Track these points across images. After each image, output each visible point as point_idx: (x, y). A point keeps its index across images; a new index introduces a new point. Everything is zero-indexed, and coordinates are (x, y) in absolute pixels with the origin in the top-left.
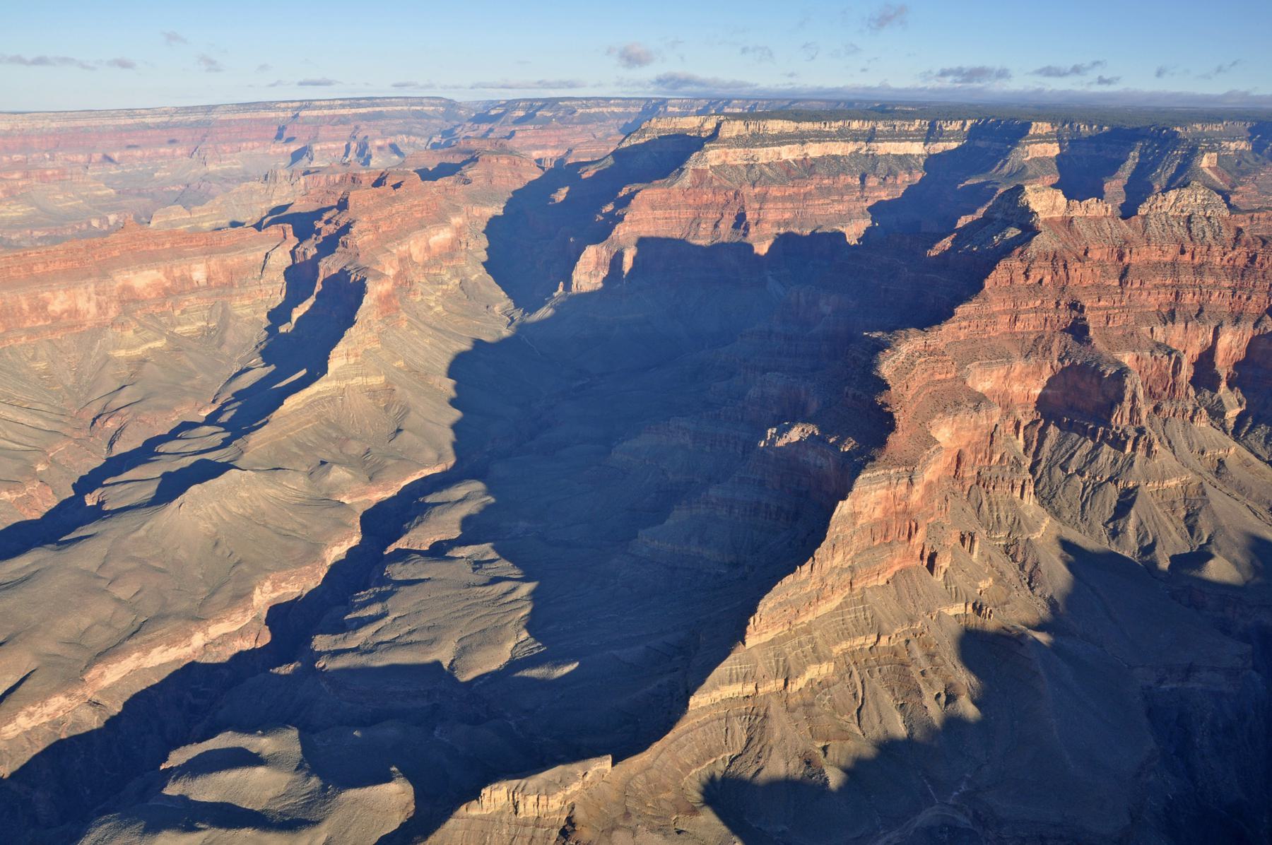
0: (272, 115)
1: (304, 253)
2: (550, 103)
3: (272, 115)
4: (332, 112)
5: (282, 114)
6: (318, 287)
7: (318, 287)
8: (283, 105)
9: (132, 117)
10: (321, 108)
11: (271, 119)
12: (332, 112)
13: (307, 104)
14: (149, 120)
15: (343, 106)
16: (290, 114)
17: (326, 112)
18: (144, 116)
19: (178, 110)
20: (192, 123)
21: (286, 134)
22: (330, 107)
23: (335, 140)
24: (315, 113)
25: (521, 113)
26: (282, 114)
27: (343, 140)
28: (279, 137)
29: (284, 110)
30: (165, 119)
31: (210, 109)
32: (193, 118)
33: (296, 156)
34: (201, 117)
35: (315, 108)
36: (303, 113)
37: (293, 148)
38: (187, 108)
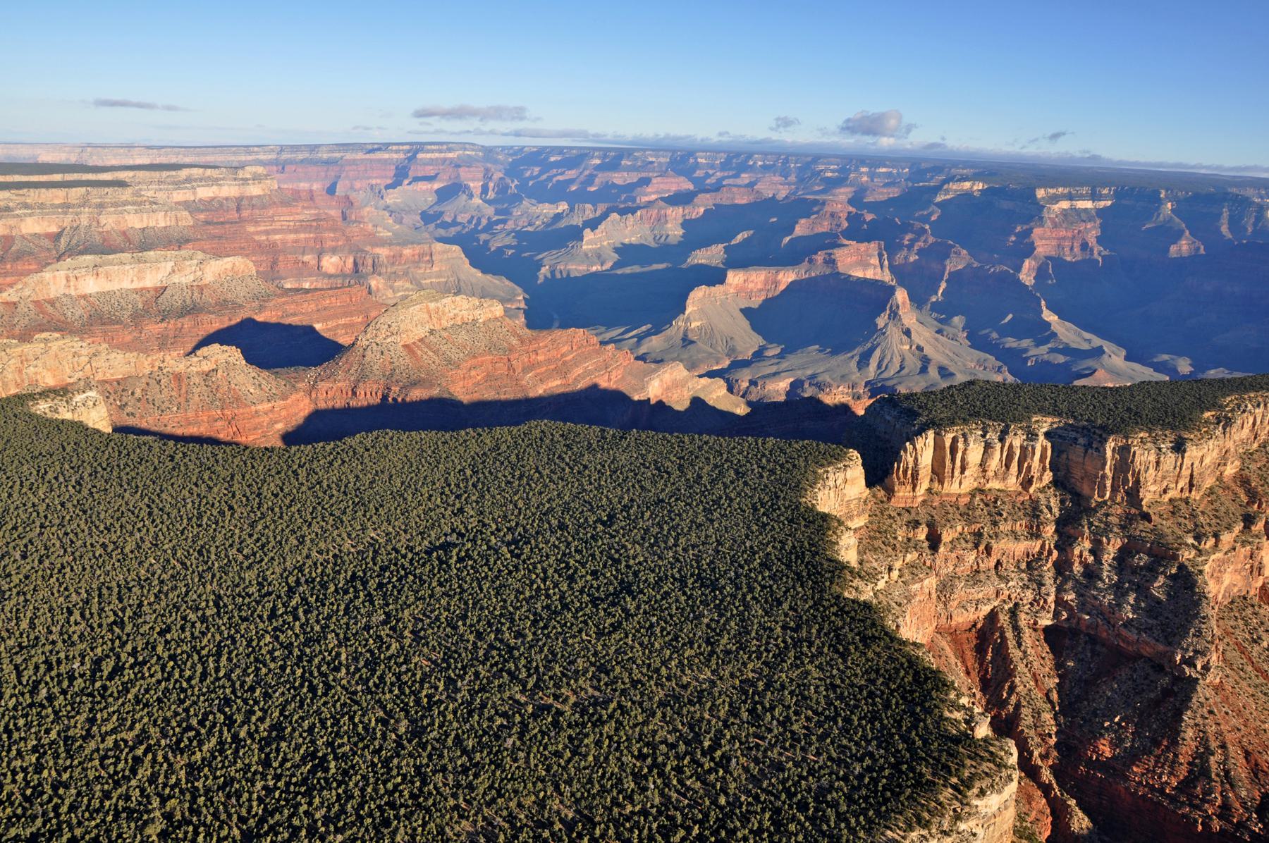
0: (386, 156)
1: (906, 258)
2: (622, 154)
3: (386, 156)
4: (442, 155)
5: (395, 156)
6: (946, 276)
7: (946, 276)
8: (394, 148)
9: (250, 153)
10: (433, 151)
11: (386, 160)
12: (442, 155)
13: (418, 147)
14: (262, 157)
15: (449, 150)
16: (402, 156)
17: (437, 155)
18: (257, 153)
19: (282, 149)
20: (302, 161)
21: (411, 174)
22: (440, 151)
23: (473, 180)
24: (429, 156)
25: (598, 162)
26: (395, 156)
27: (479, 180)
28: (401, 175)
29: (397, 152)
30: (273, 156)
31: (314, 148)
32: (300, 156)
33: (445, 195)
34: (306, 155)
35: (428, 151)
36: (420, 156)
37: (437, 186)
38: (292, 147)
